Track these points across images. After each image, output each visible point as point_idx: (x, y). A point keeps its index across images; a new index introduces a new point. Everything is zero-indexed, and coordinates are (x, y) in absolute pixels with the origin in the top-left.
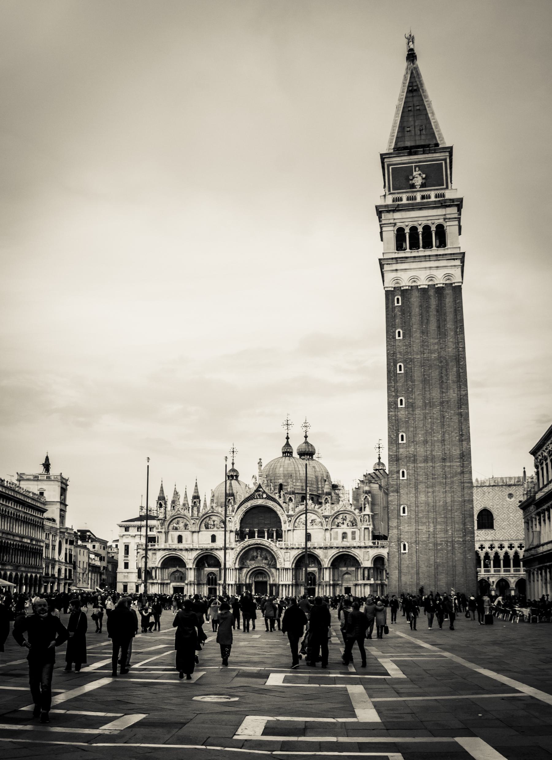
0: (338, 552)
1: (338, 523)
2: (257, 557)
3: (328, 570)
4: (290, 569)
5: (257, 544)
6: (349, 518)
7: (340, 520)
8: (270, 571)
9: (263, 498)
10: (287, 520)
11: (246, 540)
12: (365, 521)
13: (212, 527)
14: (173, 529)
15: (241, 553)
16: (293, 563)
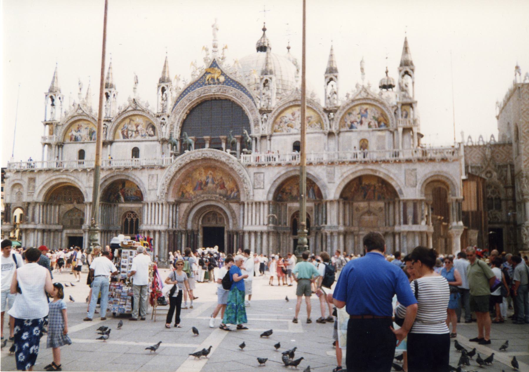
0: (354, 170)
1: (352, 123)
2: (207, 183)
3: (335, 206)
4: (264, 204)
5: (205, 159)
6: (372, 113)
7: (355, 117)
8: (229, 208)
9: (219, 83)
10: (260, 119)
11: (187, 152)
12: (404, 115)
13: (134, 134)
14: (71, 139)
15: (178, 176)
16: (269, 192)
